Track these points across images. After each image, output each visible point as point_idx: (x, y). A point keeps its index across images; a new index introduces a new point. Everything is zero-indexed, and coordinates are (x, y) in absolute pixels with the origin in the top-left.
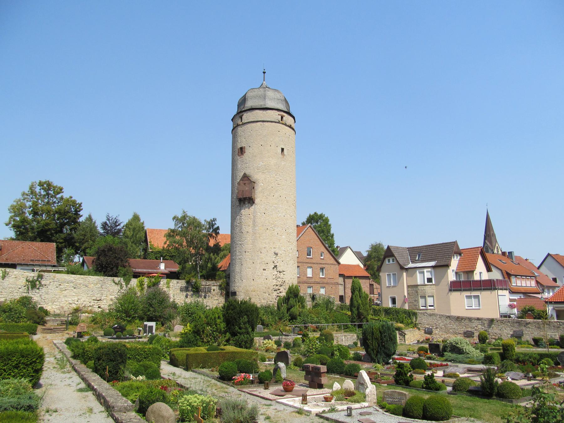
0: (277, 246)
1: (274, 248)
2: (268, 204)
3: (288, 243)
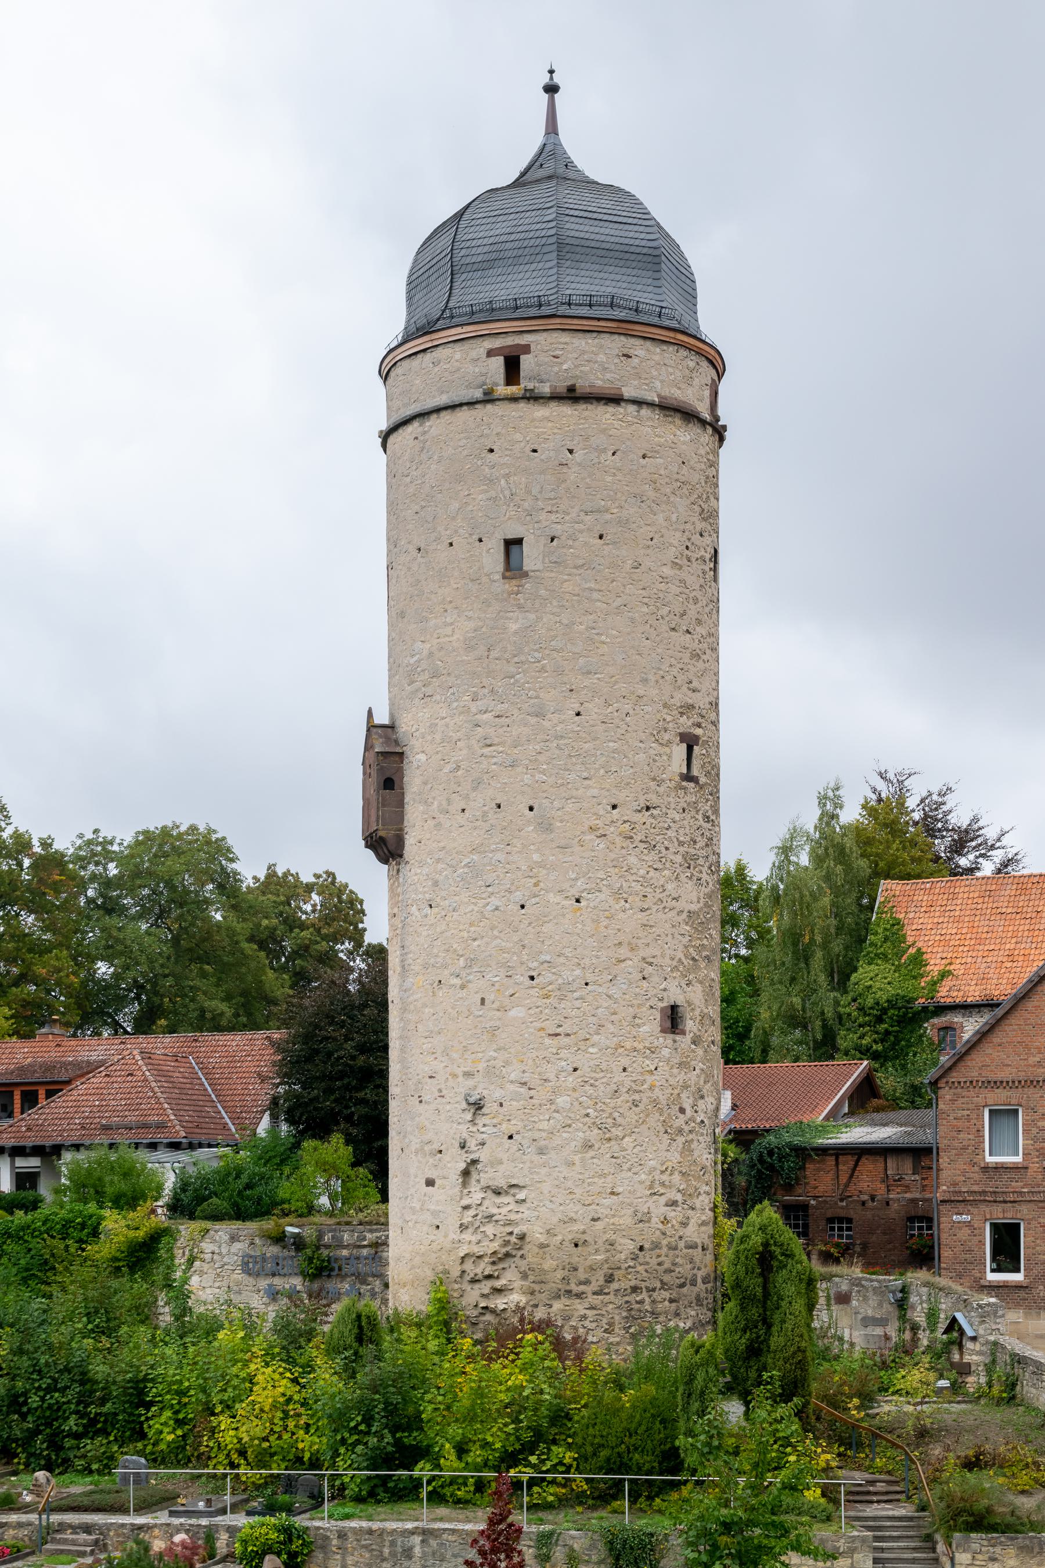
0: (481, 1066)
1: (468, 1075)
2: (442, 854)
3: (548, 1041)
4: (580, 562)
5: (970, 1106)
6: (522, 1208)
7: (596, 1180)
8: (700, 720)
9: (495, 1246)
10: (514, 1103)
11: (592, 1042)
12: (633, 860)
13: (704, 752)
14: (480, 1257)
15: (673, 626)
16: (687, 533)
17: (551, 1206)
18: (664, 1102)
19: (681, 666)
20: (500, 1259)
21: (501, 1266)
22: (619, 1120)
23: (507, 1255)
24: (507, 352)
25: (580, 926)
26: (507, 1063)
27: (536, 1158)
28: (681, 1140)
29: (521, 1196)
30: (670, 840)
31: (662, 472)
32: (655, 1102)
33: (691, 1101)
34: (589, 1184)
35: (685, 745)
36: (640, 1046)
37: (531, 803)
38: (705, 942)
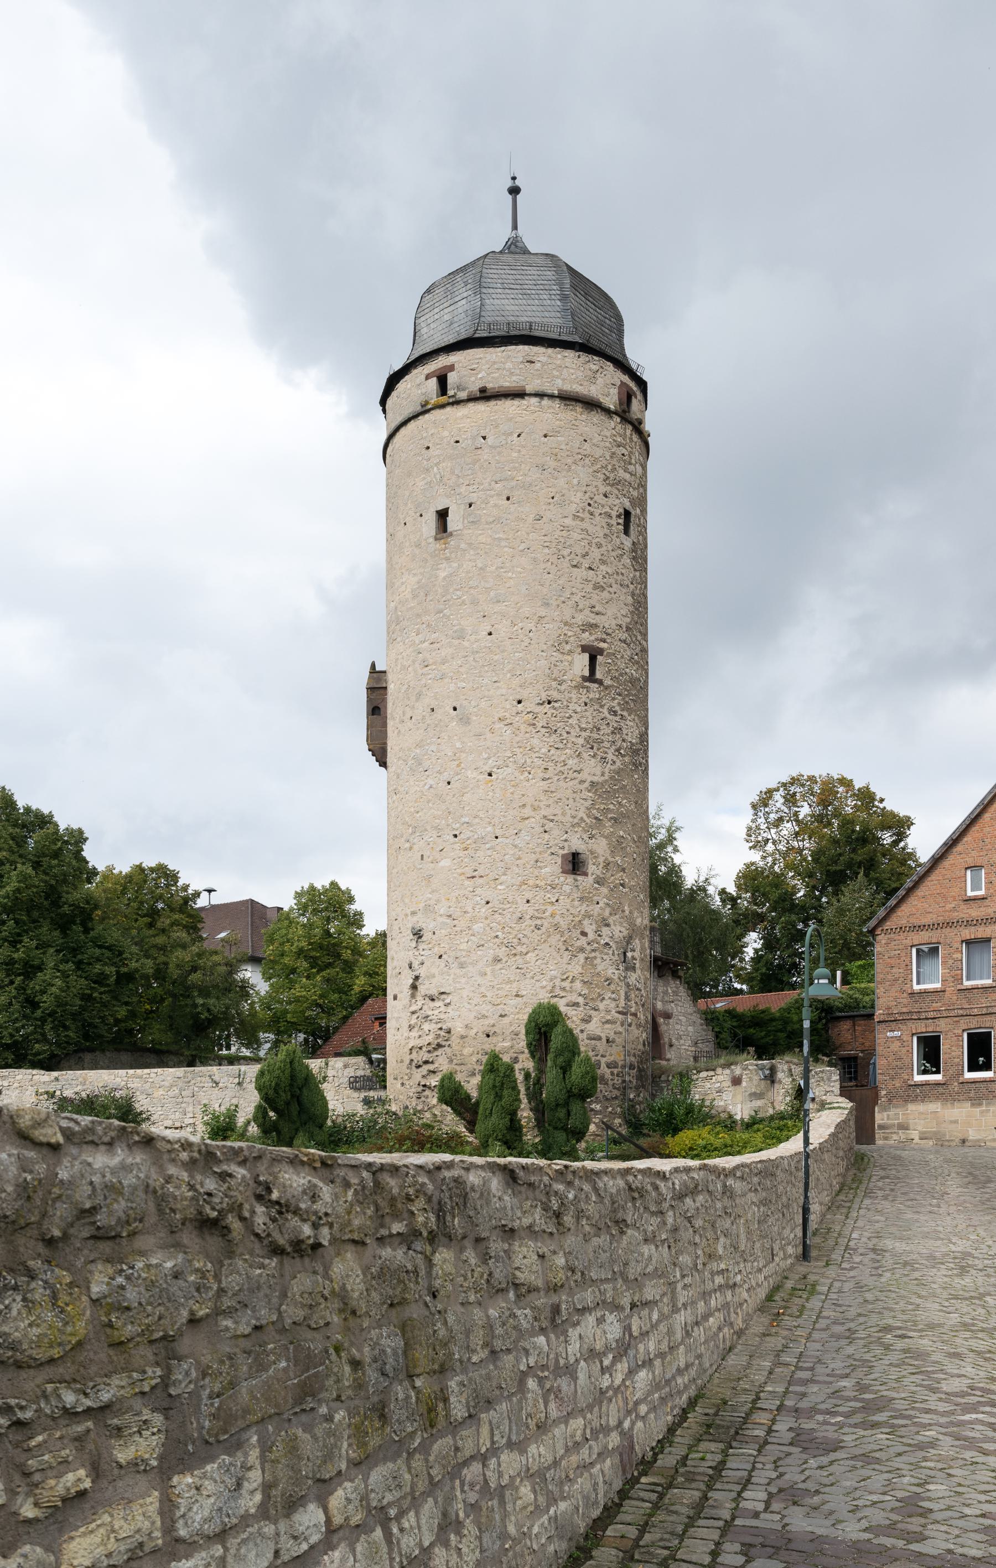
0: (421, 906)
1: (413, 913)
3: (467, 883)
4: (491, 520)
5: (901, 947)
6: (449, 1009)
7: (504, 986)
8: (604, 636)
9: (430, 1038)
10: (443, 931)
11: (500, 881)
12: (535, 742)
13: (610, 661)
14: (421, 1048)
15: (575, 563)
16: (588, 494)
17: (469, 1006)
18: (566, 927)
19: (583, 594)
20: (435, 1049)
21: (436, 1053)
22: (524, 940)
23: (439, 1046)
24: (438, 374)
25: (491, 794)
26: (438, 901)
27: (458, 971)
28: (581, 957)
29: (448, 1001)
30: (572, 726)
31: (563, 447)
32: (556, 926)
33: (594, 927)
34: (498, 989)
35: (587, 656)
36: (542, 883)
37: (454, 705)
38: (611, 807)
